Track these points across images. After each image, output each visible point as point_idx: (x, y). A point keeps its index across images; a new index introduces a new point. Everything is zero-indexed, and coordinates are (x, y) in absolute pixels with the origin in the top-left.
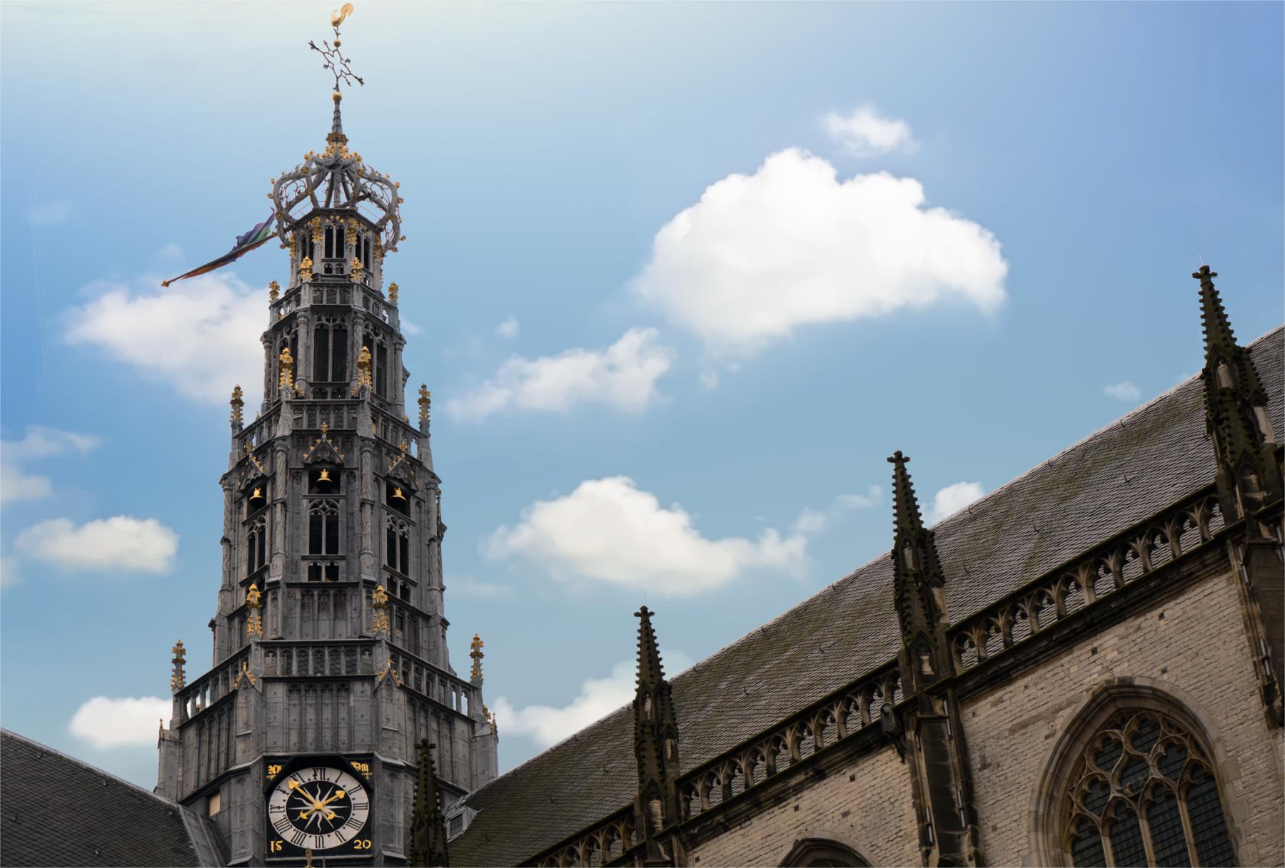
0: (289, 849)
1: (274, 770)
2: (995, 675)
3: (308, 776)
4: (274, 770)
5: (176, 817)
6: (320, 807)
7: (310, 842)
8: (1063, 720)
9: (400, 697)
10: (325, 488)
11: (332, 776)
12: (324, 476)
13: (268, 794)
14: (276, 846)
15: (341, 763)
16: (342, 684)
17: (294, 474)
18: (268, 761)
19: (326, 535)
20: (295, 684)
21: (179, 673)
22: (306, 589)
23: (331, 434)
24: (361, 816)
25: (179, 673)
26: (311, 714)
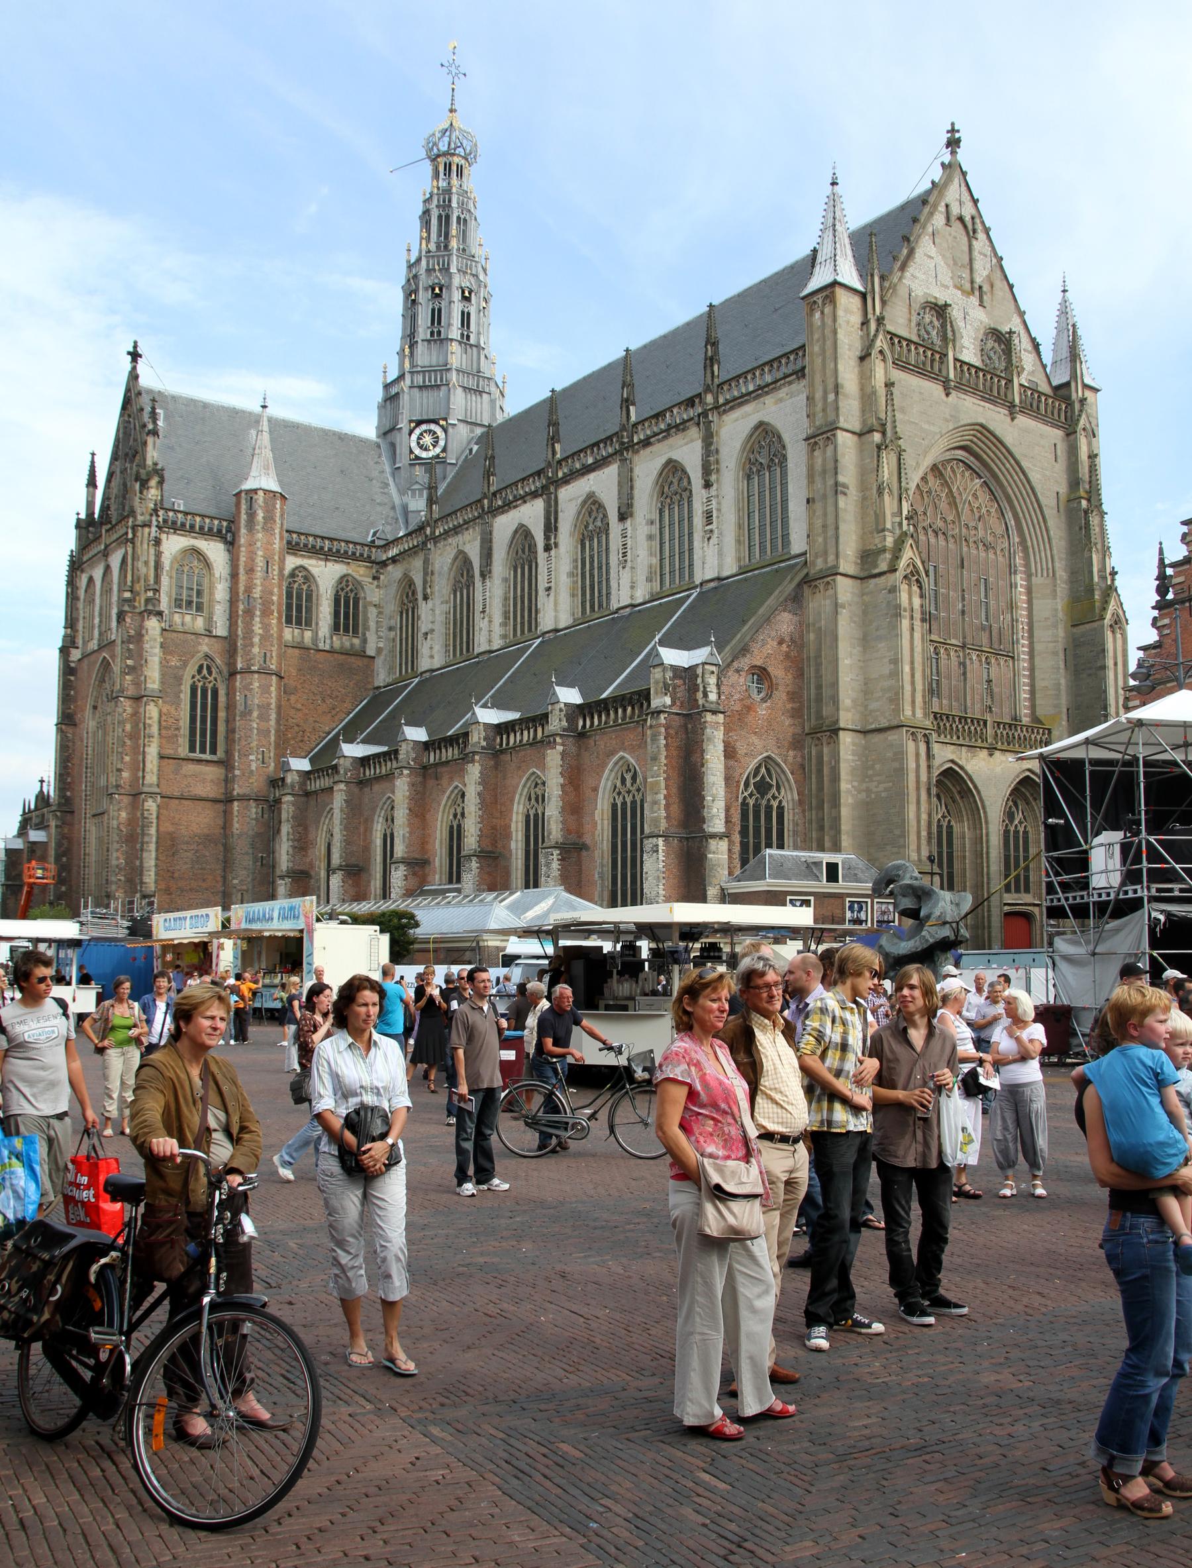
0: (417, 458)
1: (413, 425)
2: (566, 480)
3: (424, 427)
4: (413, 425)
5: (379, 446)
6: (428, 440)
7: (424, 455)
8: (580, 501)
9: (460, 390)
10: (438, 296)
11: (433, 427)
12: (437, 291)
13: (410, 435)
14: (413, 456)
15: (435, 422)
16: (438, 386)
17: (426, 289)
18: (411, 421)
19: (436, 317)
20: (420, 387)
21: (385, 377)
22: (429, 341)
23: (440, 270)
24: (442, 443)
25: (385, 377)
26: (425, 401)
